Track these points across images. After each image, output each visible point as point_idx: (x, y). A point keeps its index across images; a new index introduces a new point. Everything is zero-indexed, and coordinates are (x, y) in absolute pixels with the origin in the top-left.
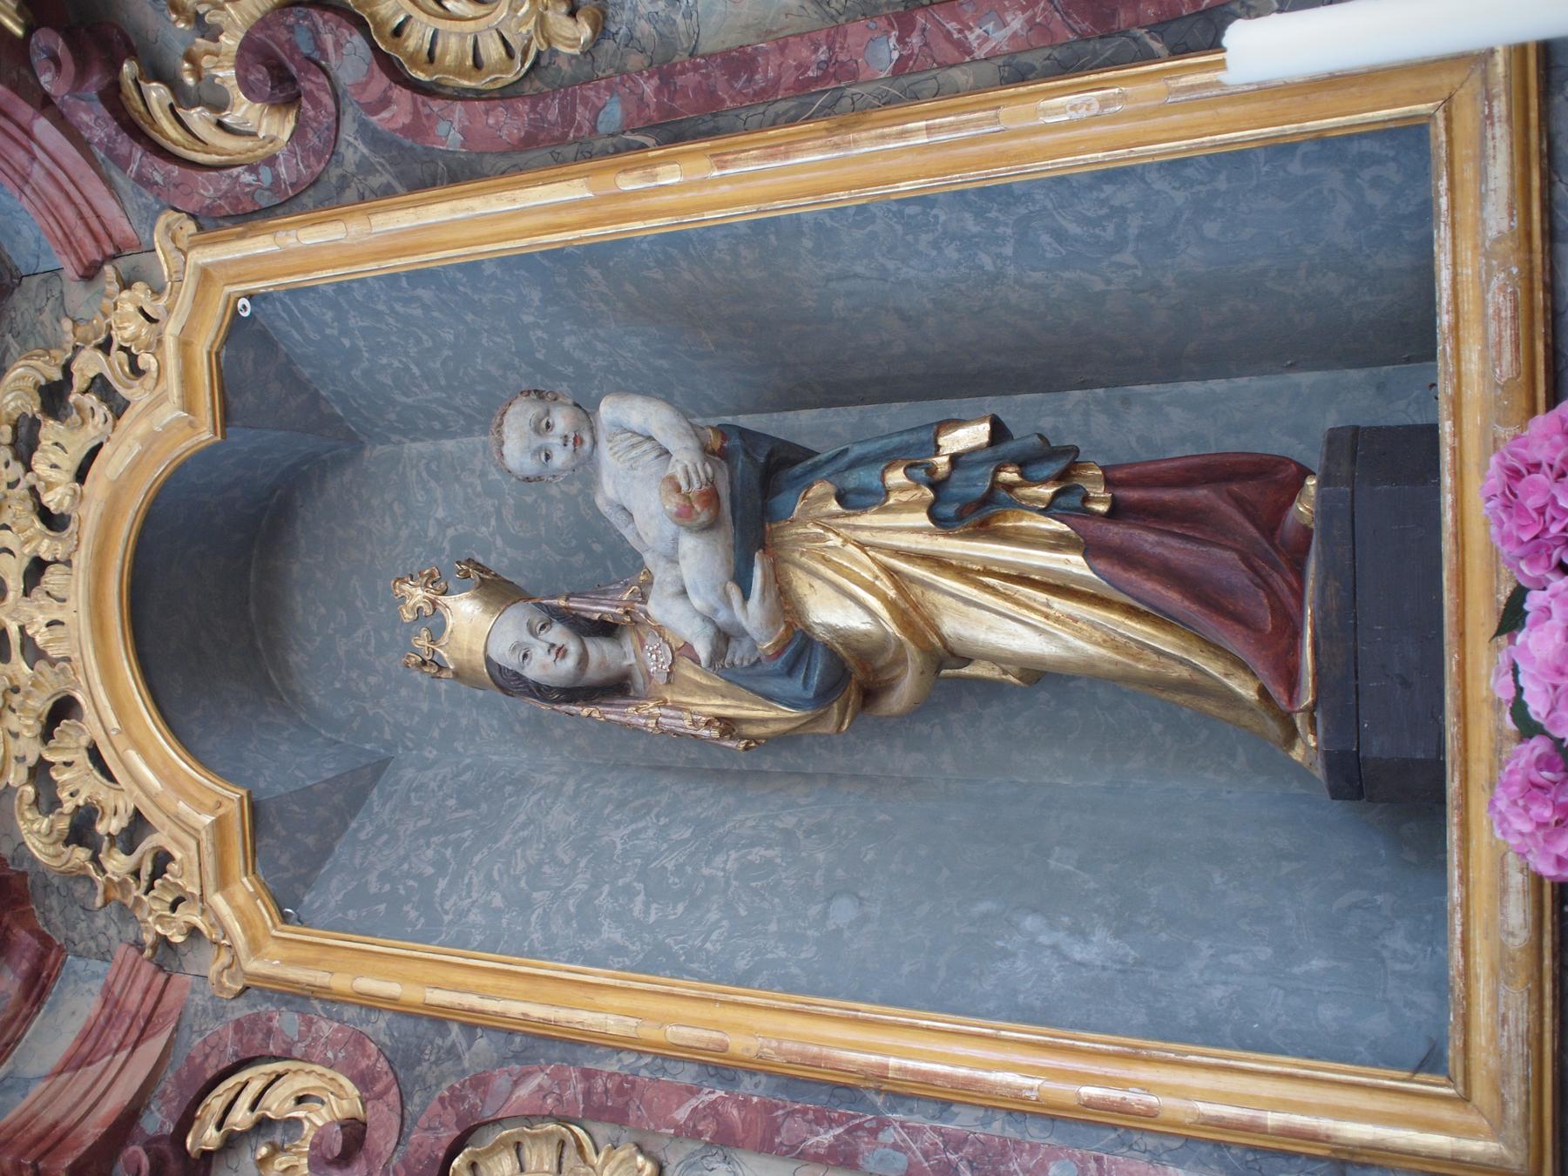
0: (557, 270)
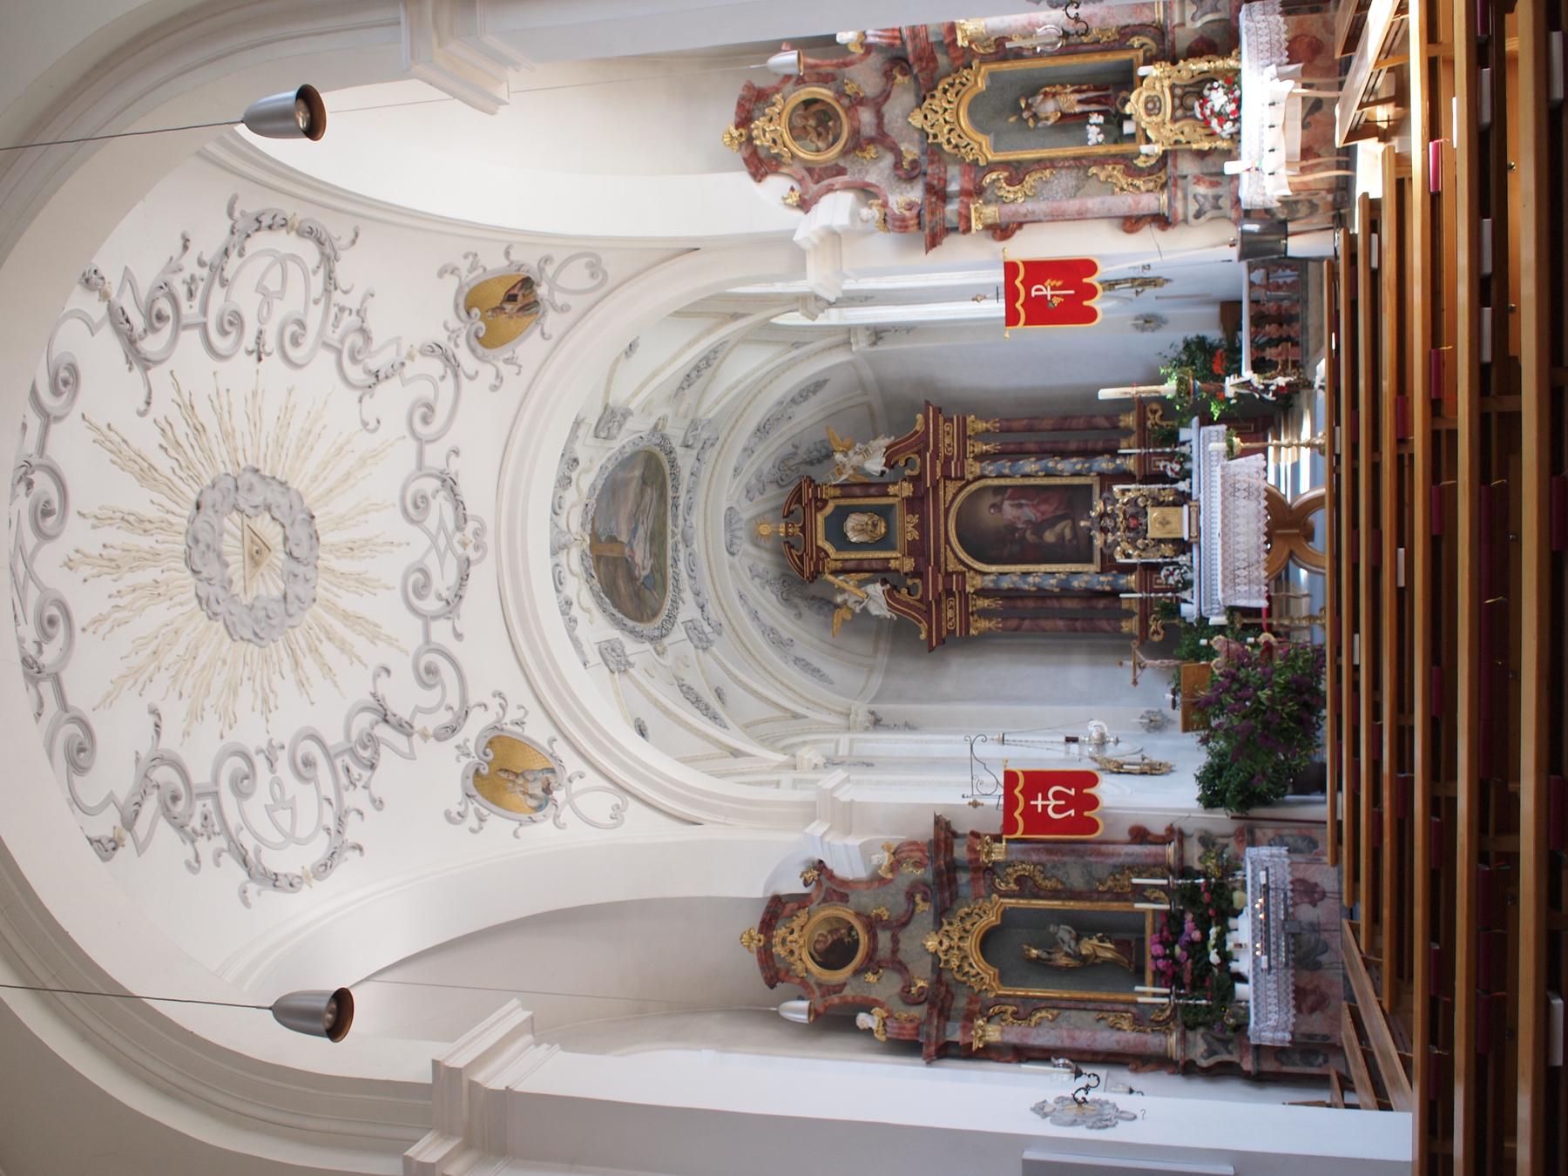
0: (1052, 911)
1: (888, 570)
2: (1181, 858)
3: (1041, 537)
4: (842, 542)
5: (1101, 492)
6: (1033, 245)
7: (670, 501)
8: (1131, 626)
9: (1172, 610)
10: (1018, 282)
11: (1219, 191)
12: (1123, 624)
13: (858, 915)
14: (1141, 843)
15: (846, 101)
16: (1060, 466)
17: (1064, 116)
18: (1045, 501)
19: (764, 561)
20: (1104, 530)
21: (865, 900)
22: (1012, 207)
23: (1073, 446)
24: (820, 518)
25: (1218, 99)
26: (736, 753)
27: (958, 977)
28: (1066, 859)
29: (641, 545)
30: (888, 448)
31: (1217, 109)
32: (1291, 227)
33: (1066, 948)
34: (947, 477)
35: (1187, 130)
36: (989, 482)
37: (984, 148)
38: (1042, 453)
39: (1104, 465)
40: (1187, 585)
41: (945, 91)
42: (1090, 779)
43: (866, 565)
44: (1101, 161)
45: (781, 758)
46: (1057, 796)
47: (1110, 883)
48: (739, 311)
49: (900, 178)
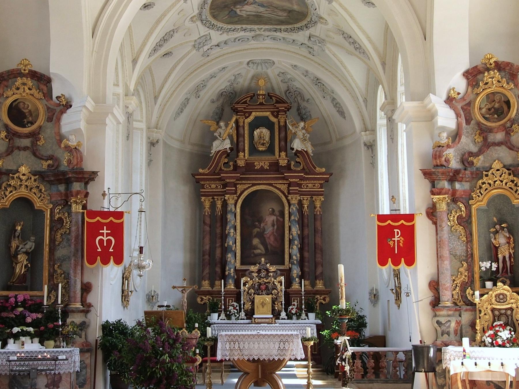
1: (238, 152)
2: (73, 311)
3: (255, 237)
4: (253, 126)
5: (280, 270)
6: (423, 231)
7: (278, 27)
8: (206, 285)
9: (215, 308)
10: (402, 221)
11: (452, 335)
12: (207, 282)
13: (40, 127)
14: (82, 289)
15: (508, 125)
16: (295, 247)
17: (496, 248)
18: (276, 239)
19: (244, 82)
20: (259, 271)
21: (49, 131)
22: (445, 219)
23: (306, 254)
24: (268, 114)
25: (505, 334)
26: (135, 61)
27: (4, 185)
28: (73, 246)
29: (254, 10)
30: (306, 152)
31: (499, 334)
32: (431, 375)
33: (21, 246)
34: (290, 185)
35: (487, 317)
36: (287, 208)
37: (479, 203)
38: (302, 238)
39: (295, 272)
40: (229, 317)
41: (513, 181)
42: (119, 260)
43: (241, 139)
44: (470, 269)
45: (132, 88)
46: (109, 241)
47: (59, 271)
48: (387, 67)
49: (463, 155)
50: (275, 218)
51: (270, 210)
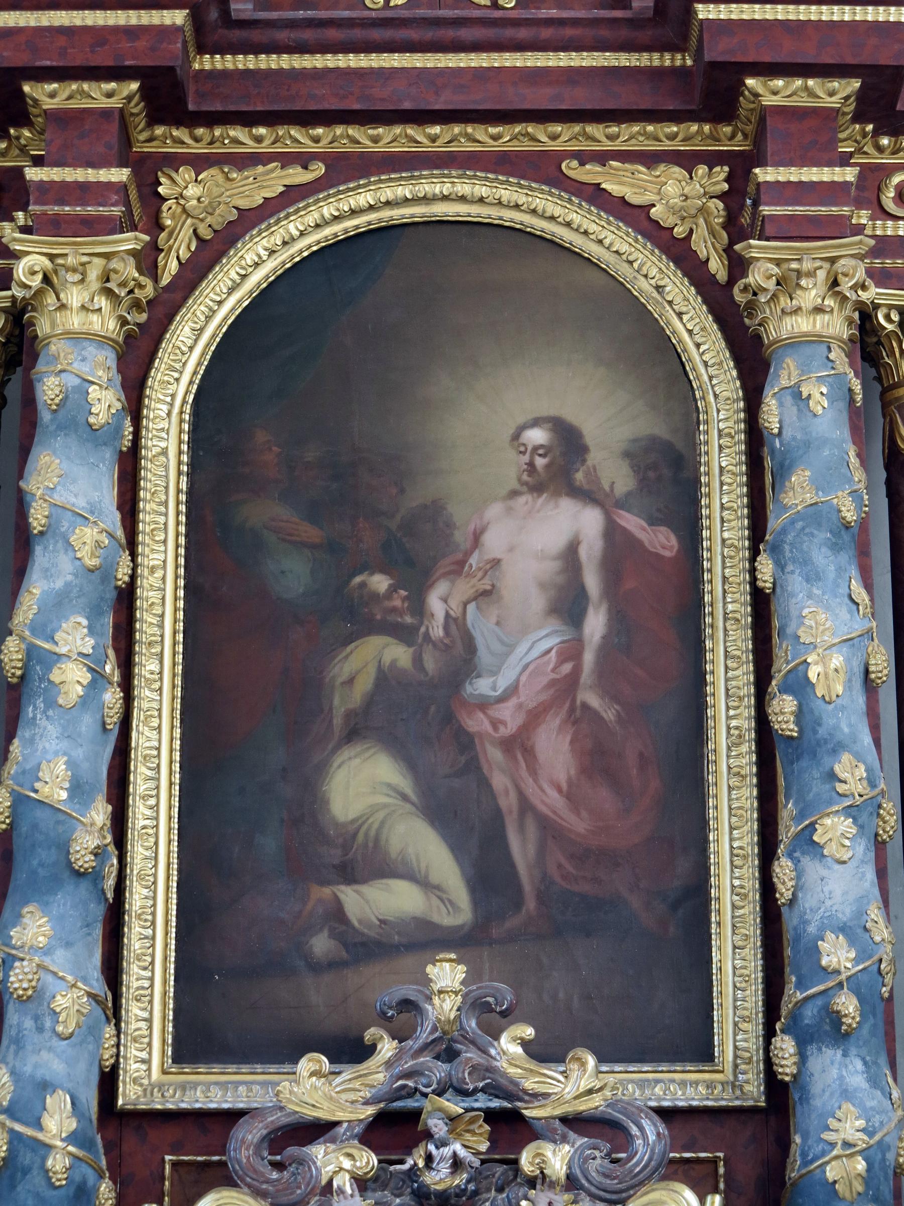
3: (355, 731)
16: (835, 830)
18: (598, 759)
20: (394, 1128)
50: (589, 523)
51: (537, 436)
